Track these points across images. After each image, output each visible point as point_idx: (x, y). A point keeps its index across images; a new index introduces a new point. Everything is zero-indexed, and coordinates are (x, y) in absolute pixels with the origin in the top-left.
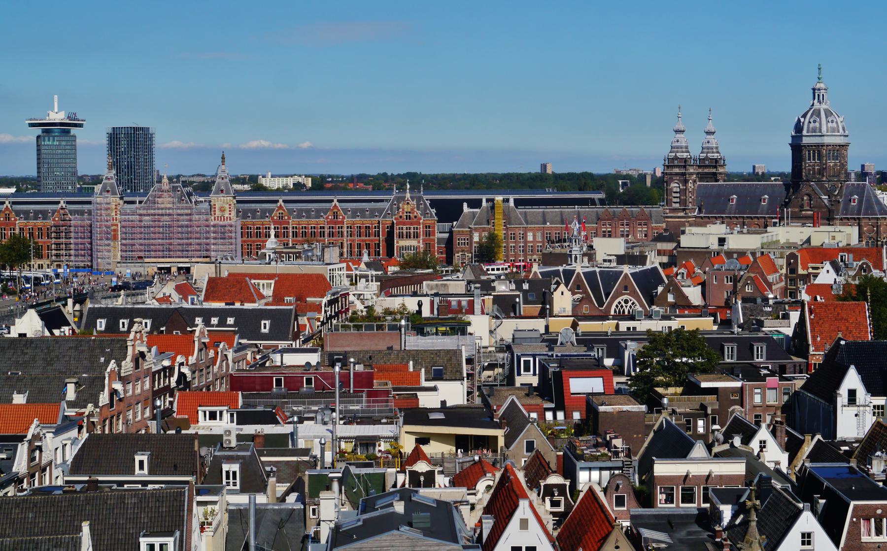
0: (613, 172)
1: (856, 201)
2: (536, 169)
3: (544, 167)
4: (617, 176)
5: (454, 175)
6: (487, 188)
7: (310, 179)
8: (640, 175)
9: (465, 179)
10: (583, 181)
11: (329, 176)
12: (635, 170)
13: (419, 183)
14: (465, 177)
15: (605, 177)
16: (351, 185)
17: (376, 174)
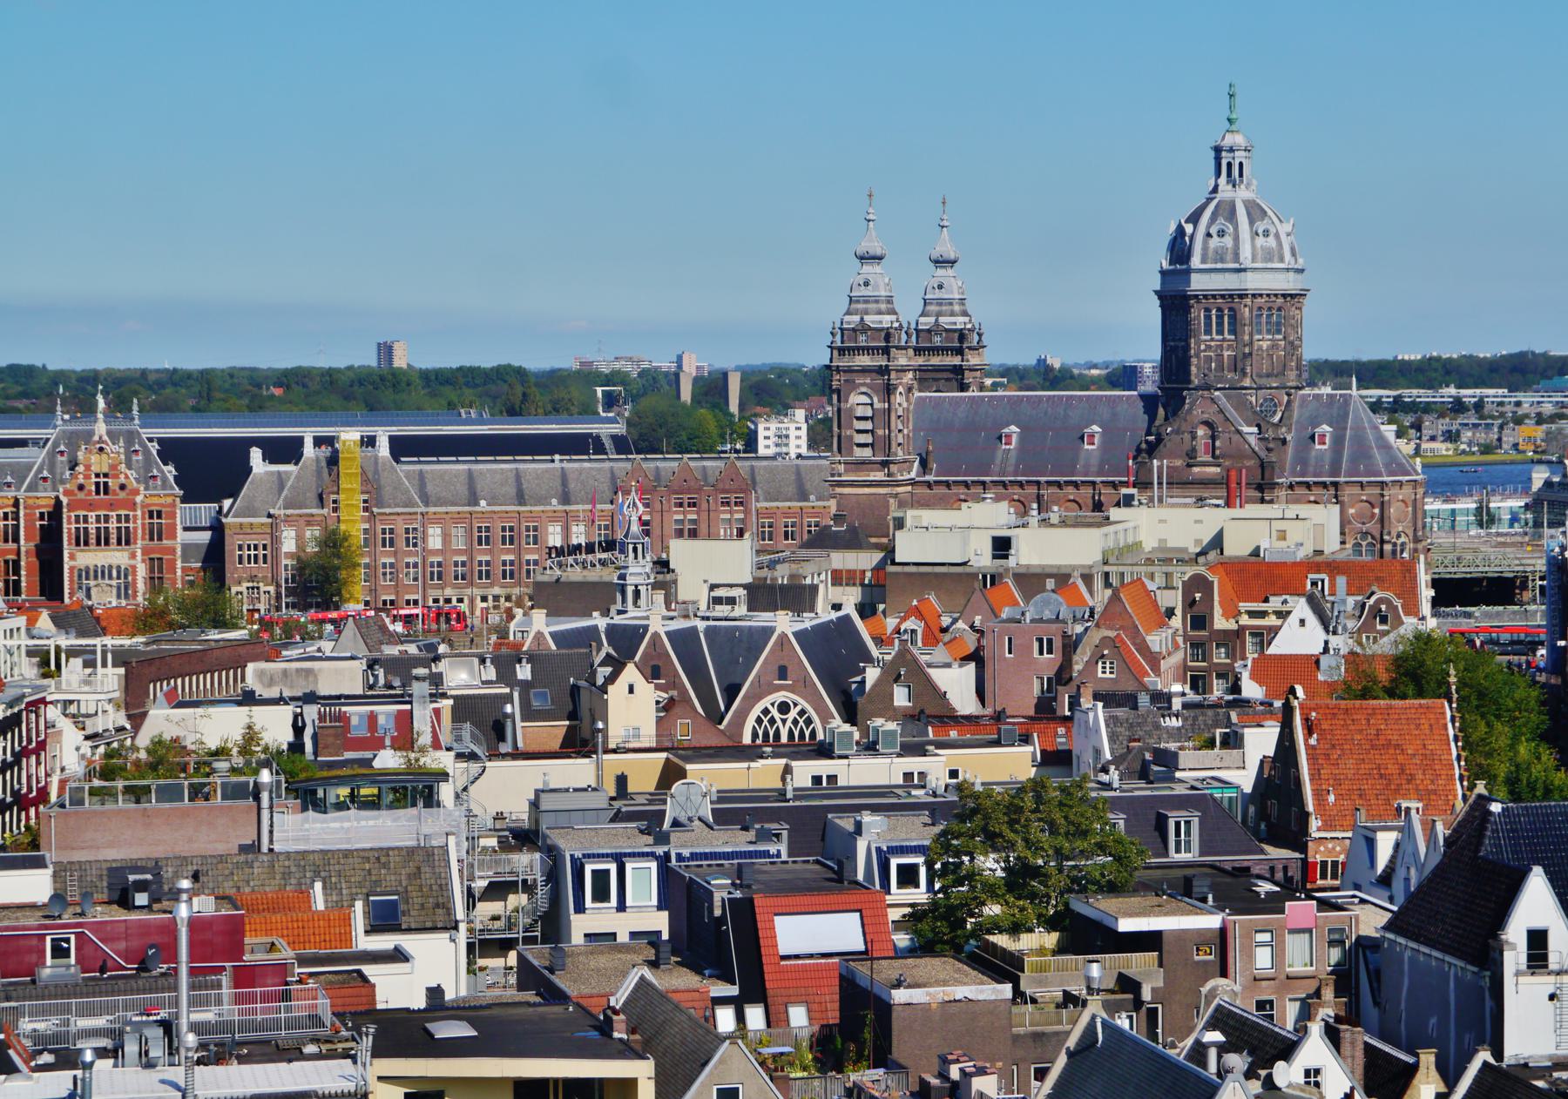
1: (1096, 440)
2: (369, 359)
3: (386, 350)
4: (588, 376)
5: (144, 373)
6: (251, 409)
8: (643, 374)
9: (175, 385)
10: (519, 390)
12: (630, 359)
13: (51, 395)
14: (176, 378)
15: (554, 378)
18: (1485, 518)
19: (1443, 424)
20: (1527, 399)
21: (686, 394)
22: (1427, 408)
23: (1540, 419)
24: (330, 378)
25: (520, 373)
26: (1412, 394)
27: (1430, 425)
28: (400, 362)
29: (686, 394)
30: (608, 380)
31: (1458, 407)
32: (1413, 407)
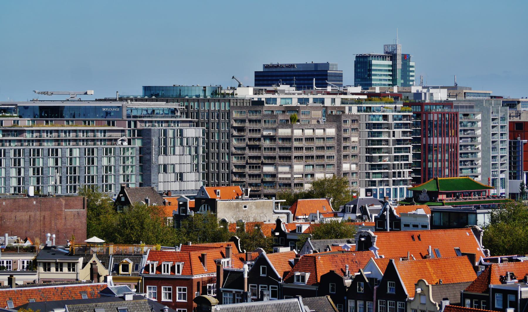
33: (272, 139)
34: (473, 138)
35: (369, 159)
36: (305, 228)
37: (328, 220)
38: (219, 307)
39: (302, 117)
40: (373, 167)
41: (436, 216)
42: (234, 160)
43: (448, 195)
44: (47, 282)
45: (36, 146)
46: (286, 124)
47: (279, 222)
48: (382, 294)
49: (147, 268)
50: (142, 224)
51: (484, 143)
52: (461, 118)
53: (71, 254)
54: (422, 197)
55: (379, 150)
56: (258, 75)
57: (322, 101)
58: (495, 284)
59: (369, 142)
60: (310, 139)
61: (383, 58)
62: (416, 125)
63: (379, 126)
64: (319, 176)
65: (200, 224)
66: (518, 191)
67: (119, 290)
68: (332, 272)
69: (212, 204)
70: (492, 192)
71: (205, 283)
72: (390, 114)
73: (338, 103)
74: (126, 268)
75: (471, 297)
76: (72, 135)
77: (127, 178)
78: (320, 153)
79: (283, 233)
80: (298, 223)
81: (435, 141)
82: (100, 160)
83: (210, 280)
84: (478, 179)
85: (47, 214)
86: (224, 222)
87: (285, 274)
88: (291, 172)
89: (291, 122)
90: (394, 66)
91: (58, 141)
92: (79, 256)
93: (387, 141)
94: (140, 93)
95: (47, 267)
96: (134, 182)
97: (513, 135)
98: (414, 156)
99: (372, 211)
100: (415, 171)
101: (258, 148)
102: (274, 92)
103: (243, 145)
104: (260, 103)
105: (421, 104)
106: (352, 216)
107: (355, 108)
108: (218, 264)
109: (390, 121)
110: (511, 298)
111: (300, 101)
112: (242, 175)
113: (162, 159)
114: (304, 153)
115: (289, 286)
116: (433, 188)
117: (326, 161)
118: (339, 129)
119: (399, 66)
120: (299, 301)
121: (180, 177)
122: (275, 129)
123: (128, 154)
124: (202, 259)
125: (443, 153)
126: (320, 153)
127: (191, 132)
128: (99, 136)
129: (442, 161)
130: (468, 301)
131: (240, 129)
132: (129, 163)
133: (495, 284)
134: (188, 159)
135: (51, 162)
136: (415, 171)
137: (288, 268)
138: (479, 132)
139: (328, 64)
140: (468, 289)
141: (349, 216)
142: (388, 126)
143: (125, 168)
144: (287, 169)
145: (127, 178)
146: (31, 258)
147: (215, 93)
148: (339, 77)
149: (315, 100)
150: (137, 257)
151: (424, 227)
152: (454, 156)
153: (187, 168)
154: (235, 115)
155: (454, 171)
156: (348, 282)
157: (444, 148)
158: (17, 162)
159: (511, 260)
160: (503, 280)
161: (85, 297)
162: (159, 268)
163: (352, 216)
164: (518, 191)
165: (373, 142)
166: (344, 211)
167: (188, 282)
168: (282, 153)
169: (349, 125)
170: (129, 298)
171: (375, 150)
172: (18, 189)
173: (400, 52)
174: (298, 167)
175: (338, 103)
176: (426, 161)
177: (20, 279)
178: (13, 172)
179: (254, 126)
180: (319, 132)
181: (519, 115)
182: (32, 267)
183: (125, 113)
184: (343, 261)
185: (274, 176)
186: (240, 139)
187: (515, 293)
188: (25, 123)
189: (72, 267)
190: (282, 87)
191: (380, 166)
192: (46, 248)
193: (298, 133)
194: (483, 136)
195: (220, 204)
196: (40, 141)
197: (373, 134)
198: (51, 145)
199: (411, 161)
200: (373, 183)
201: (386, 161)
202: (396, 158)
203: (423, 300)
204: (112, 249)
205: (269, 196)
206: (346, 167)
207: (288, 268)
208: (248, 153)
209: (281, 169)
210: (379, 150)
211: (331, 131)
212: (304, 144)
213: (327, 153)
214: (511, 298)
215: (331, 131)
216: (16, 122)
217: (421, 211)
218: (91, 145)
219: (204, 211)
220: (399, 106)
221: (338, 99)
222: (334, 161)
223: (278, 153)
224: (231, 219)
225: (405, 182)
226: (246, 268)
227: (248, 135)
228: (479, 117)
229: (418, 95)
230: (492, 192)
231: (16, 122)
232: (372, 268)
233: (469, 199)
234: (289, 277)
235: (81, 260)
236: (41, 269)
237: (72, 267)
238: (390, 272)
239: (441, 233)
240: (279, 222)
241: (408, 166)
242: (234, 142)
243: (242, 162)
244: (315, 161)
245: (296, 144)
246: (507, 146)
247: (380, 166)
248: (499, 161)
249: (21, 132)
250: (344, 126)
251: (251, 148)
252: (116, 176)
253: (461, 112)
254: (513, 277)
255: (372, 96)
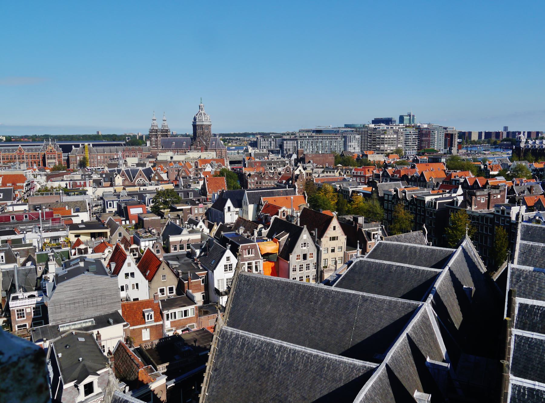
0: (123, 134)
2: (96, 134)
3: (98, 132)
4: (125, 136)
5: (64, 135)
7: (4, 137)
11: (12, 136)
14: (68, 136)
15: (121, 136)
16: (22, 140)
17: (32, 135)
18: (238, 153)
19: (235, 141)
20: (245, 138)
21: (138, 138)
22: (233, 139)
23: (247, 141)
24: (89, 136)
25: (116, 135)
26: (231, 138)
27: (234, 142)
28: (100, 134)
29: (138, 138)
30: (128, 136)
31: (237, 139)
32: (232, 139)
33: (379, 138)
34: (434, 138)
35: (405, 144)
36: (392, 162)
37: (398, 160)
38: (379, 184)
39: (387, 132)
40: (406, 146)
41: (430, 159)
42: (369, 144)
43: (428, 153)
44: (327, 176)
45: (317, 140)
46: (383, 134)
47: (385, 160)
48: (419, 180)
49: (354, 173)
50: (349, 161)
51: (437, 139)
52: (431, 132)
53: (333, 169)
54: (420, 154)
55: (408, 141)
56: (373, 121)
57: (393, 128)
58: (453, 178)
59: (405, 139)
60: (389, 138)
61: (407, 116)
62: (418, 134)
63: (408, 135)
64: (392, 148)
65: (364, 161)
66: (446, 152)
67: (348, 179)
68: (405, 174)
69: (367, 156)
70: (439, 152)
71: (369, 177)
72: (412, 131)
73: (397, 128)
74: (348, 173)
75: (446, 182)
76: (326, 138)
77: (340, 149)
78: (392, 142)
79: (386, 164)
80: (390, 161)
81: (424, 139)
82: (333, 144)
83: (371, 176)
84: (436, 149)
85: (324, 158)
86: (370, 160)
87: (392, 175)
88: (384, 147)
89: (384, 134)
90: (410, 118)
91: (323, 139)
92: (335, 169)
93: (410, 139)
94: (344, 126)
95: (327, 172)
96: (342, 149)
97: (445, 137)
98: (418, 143)
99: (411, 158)
100: (418, 147)
101: (375, 141)
102: (380, 125)
103: (371, 140)
104: (376, 128)
105: (420, 129)
106: (405, 159)
107: (402, 130)
108: (373, 172)
109: (412, 133)
110: (458, 182)
111: (387, 128)
112: (371, 148)
113: (350, 144)
114: (388, 142)
115: (393, 178)
116: (423, 152)
117: (394, 144)
118: (397, 135)
119: (411, 118)
120: (400, 182)
121: (355, 148)
122: (380, 136)
123: (341, 142)
124: (368, 170)
125: (426, 142)
126: (392, 142)
127: (357, 136)
128: (333, 138)
129: (426, 144)
130: (444, 183)
131: (370, 136)
132: (341, 145)
133: (453, 178)
134: (356, 144)
135: (321, 145)
136: (418, 147)
137: (392, 173)
138: (436, 136)
139: (392, 118)
140: (445, 179)
141: (403, 159)
142: (411, 135)
143: (340, 146)
144: (383, 146)
145: (340, 149)
146: (323, 170)
147: (363, 126)
148: (395, 121)
149: (391, 128)
150: (351, 170)
151: (426, 162)
152: (429, 143)
153: (356, 146)
154: (369, 132)
155: (429, 147)
156: (410, 177)
157: (426, 140)
158: (312, 145)
159: (454, 172)
160: (455, 177)
161: (339, 180)
162: (357, 173)
163: (405, 159)
164: (446, 152)
165: (407, 139)
166: (402, 158)
167: (365, 177)
168: (382, 142)
169: (400, 134)
170: (351, 181)
171: (407, 141)
172: (317, 152)
173: (412, 115)
174: (386, 146)
175: (397, 128)
176: (421, 144)
177: (321, 175)
178: (311, 147)
179: (374, 135)
180: (392, 136)
181: (447, 131)
182: (323, 172)
183: (340, 131)
184: (408, 171)
185: (379, 148)
186: (370, 138)
187: (459, 181)
188: (314, 134)
189: (334, 172)
190: (382, 124)
191: (408, 146)
192: (326, 167)
193: (386, 136)
194: (437, 137)
195: (369, 156)
196: (318, 139)
197: (407, 137)
198: (321, 140)
199: (417, 144)
200: (406, 150)
201: (410, 144)
202: (413, 143)
203: (431, 182)
204: (344, 168)
205: (382, 154)
206: (399, 146)
207: (392, 173)
208: (373, 142)
209: (381, 146)
210: (408, 141)
211: (395, 136)
212: (388, 140)
213: (394, 142)
214: (458, 182)
215: (395, 136)
216: (312, 134)
217: (425, 158)
218: (331, 140)
219: (364, 158)
220: (414, 129)
221: (397, 127)
222: (396, 144)
223: (381, 142)
224: (372, 160)
225: (415, 150)
226: (381, 173)
227: (373, 137)
228: (436, 132)
229: (419, 126)
230: (439, 152)
231: (312, 134)
232: (416, 173)
233: (433, 154)
234: (393, 175)
235: (336, 170)
236: (325, 173)
237: (334, 172)
238: (422, 174)
239: (434, 164)
240: (385, 160)
241: (416, 145)
242: (369, 139)
243: (371, 145)
244: (391, 144)
245: (386, 140)
246: (444, 140)
247: (408, 146)
248: (441, 144)
249: (313, 137)
250: (399, 135)
251: (373, 141)
252: (338, 148)
253: (431, 130)
254: (458, 176)
255: (406, 126)
